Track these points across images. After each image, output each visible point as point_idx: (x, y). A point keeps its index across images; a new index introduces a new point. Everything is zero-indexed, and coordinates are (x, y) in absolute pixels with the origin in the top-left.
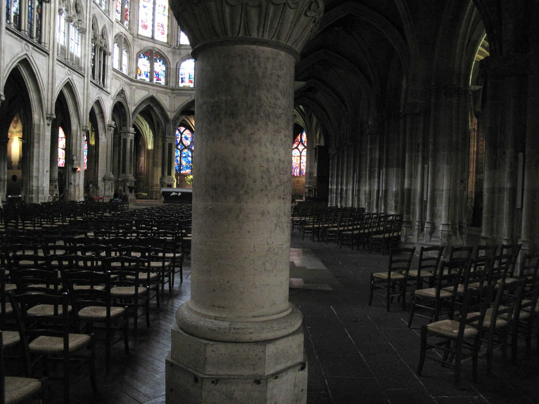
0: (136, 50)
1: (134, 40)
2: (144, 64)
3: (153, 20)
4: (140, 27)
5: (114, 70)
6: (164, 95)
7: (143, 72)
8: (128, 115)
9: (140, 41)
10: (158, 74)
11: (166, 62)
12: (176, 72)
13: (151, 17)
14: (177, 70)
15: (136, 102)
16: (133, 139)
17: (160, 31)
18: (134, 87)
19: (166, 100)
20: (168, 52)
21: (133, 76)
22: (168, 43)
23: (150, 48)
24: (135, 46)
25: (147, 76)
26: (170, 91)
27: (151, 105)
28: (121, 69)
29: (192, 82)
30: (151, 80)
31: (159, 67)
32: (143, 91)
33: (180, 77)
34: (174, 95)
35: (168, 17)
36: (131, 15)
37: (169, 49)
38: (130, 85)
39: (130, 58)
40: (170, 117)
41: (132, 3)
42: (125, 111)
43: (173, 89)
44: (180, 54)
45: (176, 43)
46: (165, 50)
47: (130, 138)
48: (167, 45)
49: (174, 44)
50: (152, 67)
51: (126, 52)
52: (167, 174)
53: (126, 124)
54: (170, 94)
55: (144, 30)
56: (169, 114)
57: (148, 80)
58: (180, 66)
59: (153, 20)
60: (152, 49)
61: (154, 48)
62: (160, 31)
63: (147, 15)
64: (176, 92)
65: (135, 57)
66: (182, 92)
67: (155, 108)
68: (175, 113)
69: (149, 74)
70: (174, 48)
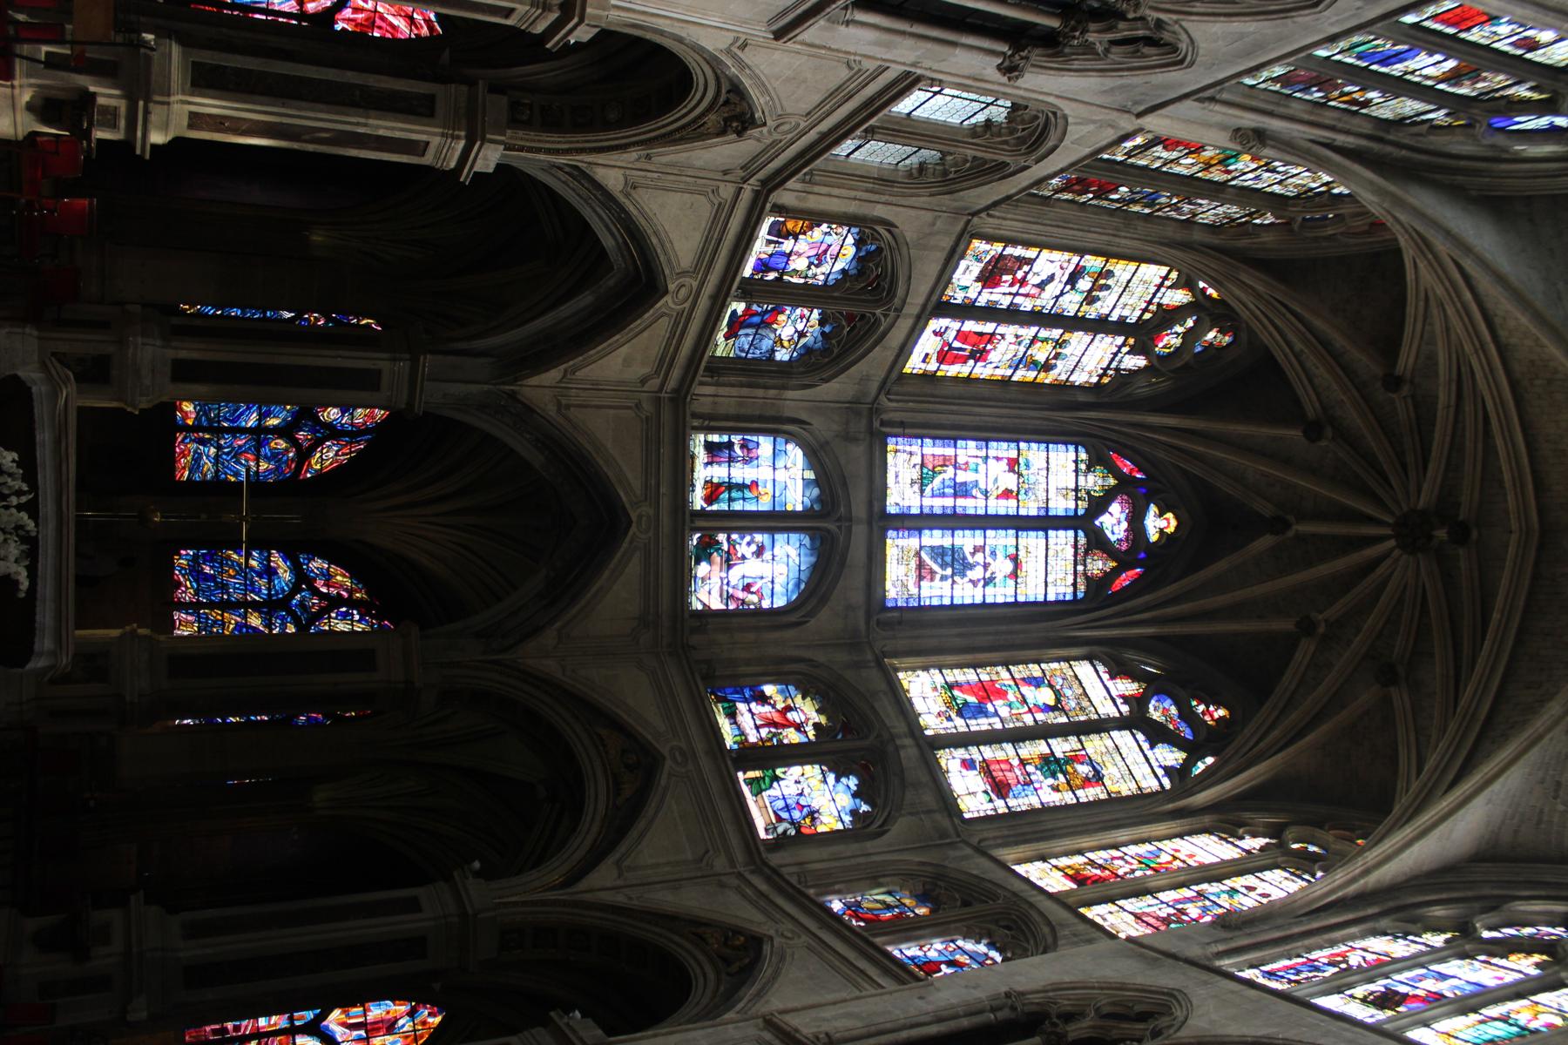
0: (910, 218)
1: (957, 212)
2: (822, 252)
3: (1012, 315)
4: (998, 247)
5: (906, 83)
6: (655, 352)
7: (787, 245)
8: (579, 140)
9: (947, 243)
10: (766, 323)
11: (814, 362)
12: (761, 418)
13: (1026, 305)
14: (777, 425)
15: (642, 196)
16: (428, 159)
17: (956, 344)
18: (727, 192)
19: (627, 362)
20: (866, 379)
21: (785, 197)
22: (903, 377)
23: (900, 292)
24: (929, 216)
25: (763, 266)
26: (672, 383)
27: (611, 282)
28: (871, 134)
29: (710, 499)
30: (750, 290)
31: (794, 328)
32: (697, 239)
33: (736, 439)
34: (648, 407)
35: (1006, 382)
36: (1072, 213)
37: (874, 386)
38: (749, 169)
39: (882, 181)
40: (534, 381)
41: (1116, 221)
42: (607, 126)
43: (680, 397)
44: (848, 438)
45: (897, 416)
46: (873, 365)
47: (435, 141)
48: (894, 375)
49: (892, 408)
50: (806, 295)
51: (922, 167)
52: (183, 354)
53: (527, 125)
54: (654, 383)
55: (976, 269)
56: (552, 376)
57: (747, 271)
58: (790, 437)
59: (1012, 315)
60: (897, 301)
61: (899, 310)
62: (956, 344)
63: (1041, 286)
64: (667, 415)
65: (880, 211)
66: (666, 451)
67: (585, 299)
68: (551, 410)
69: (771, 276)
70: (874, 410)
